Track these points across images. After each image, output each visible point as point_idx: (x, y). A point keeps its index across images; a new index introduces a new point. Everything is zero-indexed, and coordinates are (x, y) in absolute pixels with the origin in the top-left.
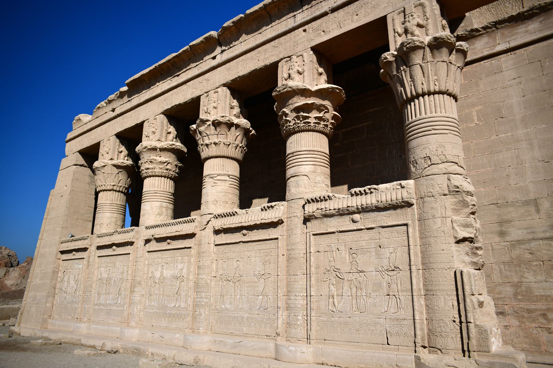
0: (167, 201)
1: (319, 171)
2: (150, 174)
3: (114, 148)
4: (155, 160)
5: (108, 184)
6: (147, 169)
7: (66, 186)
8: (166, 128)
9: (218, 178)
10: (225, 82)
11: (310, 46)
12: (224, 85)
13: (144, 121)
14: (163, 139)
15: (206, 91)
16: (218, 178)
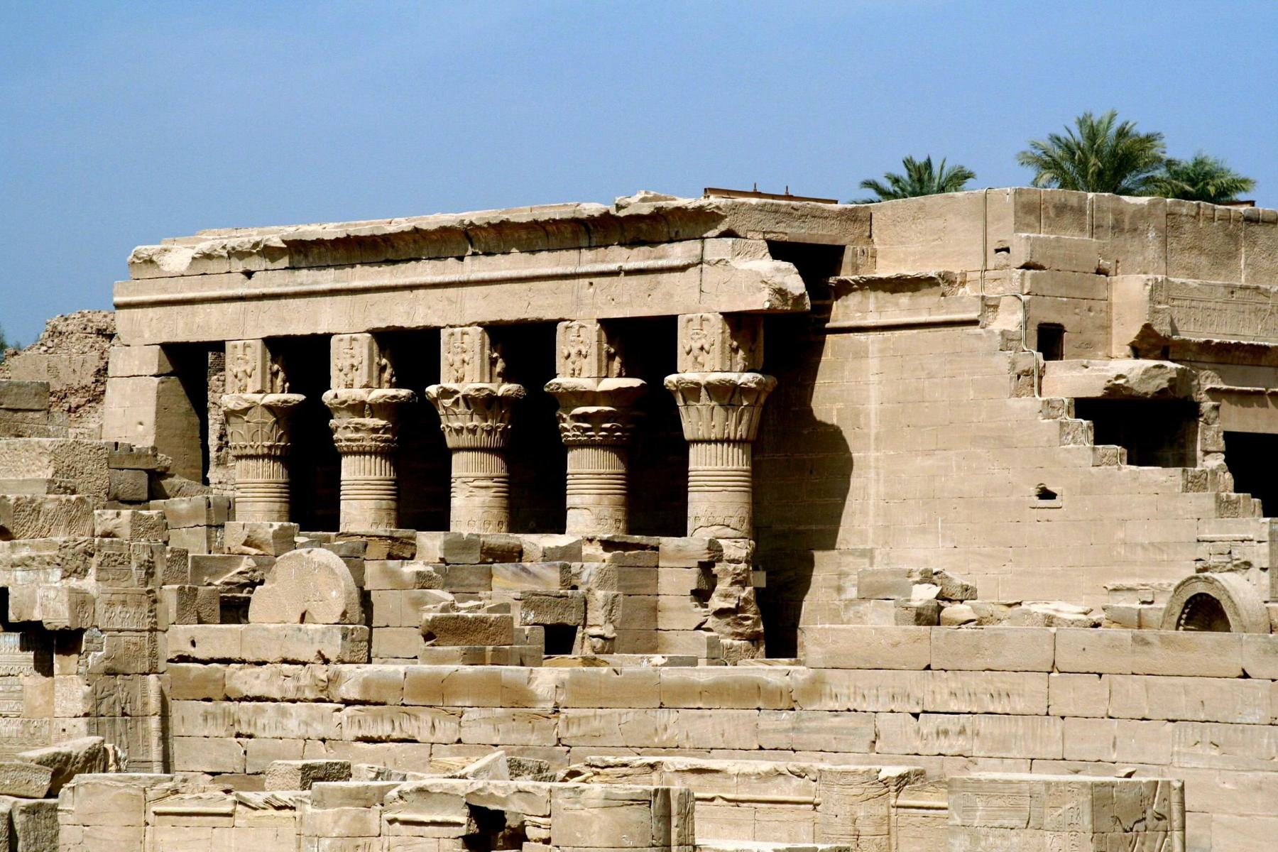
0: (390, 497)
1: (606, 502)
2: (355, 449)
3: (264, 366)
4: (364, 425)
5: (259, 443)
6: (348, 440)
7: (141, 424)
8: (377, 359)
9: (476, 483)
10: (480, 321)
11: (596, 317)
12: (480, 324)
13: (332, 334)
14: (374, 383)
15: (451, 324)
16: (476, 483)
